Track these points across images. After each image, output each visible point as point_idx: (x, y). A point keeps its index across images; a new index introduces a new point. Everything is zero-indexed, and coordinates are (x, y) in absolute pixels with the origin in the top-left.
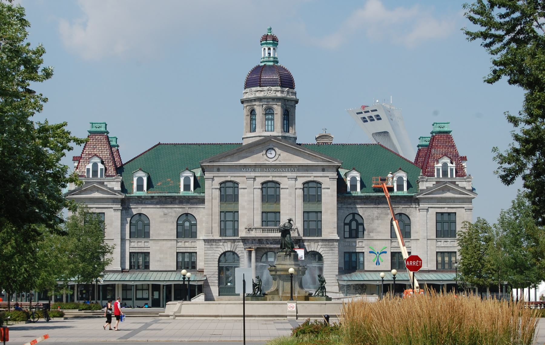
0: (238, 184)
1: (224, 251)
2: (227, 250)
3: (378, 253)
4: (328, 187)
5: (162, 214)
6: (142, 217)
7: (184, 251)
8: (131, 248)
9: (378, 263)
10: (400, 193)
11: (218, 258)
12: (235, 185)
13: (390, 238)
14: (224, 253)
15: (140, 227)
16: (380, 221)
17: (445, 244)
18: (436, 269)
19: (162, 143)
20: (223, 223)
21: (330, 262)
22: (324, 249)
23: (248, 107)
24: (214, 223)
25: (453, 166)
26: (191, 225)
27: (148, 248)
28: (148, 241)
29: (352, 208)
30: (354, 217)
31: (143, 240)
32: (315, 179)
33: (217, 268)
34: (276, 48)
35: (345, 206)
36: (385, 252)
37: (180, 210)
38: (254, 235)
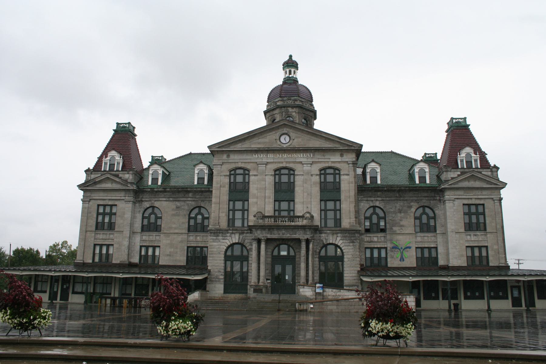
0: (249, 171)
1: (232, 243)
2: (234, 242)
3: (402, 248)
4: (347, 173)
5: (174, 207)
6: (156, 209)
7: (195, 245)
8: (142, 242)
9: (402, 259)
10: (423, 185)
11: (224, 250)
12: (246, 172)
13: (414, 232)
14: (232, 245)
15: (153, 219)
16: (402, 214)
17: (473, 238)
18: (466, 265)
19: (193, 153)
20: (231, 212)
21: (350, 256)
22: (344, 241)
23: (270, 117)
24: (222, 213)
25: (477, 157)
26: (204, 218)
27: (159, 242)
28: (159, 234)
29: (372, 201)
30: (374, 210)
31: (155, 234)
32: (333, 165)
33: (223, 262)
34: (296, 71)
35: (366, 199)
36: (410, 248)
37: (193, 203)
38: (263, 224)
